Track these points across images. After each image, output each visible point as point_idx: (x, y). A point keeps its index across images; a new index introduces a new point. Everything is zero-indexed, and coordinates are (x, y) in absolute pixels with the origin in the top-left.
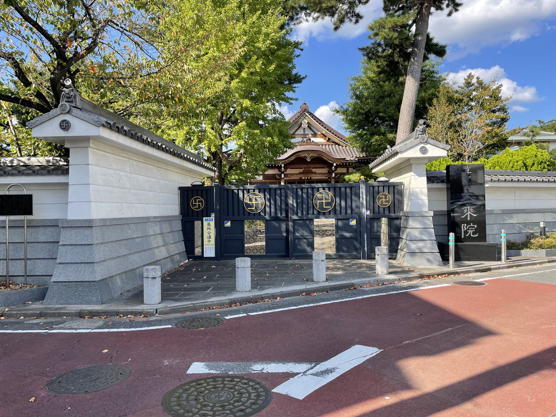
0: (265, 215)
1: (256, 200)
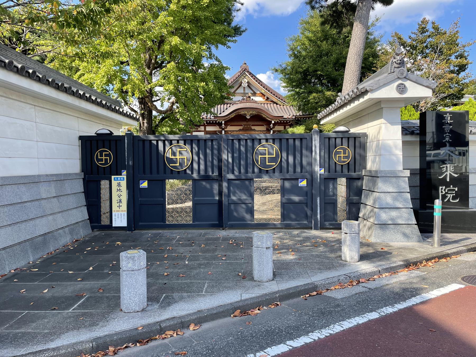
0: (192, 173)
1: (180, 153)
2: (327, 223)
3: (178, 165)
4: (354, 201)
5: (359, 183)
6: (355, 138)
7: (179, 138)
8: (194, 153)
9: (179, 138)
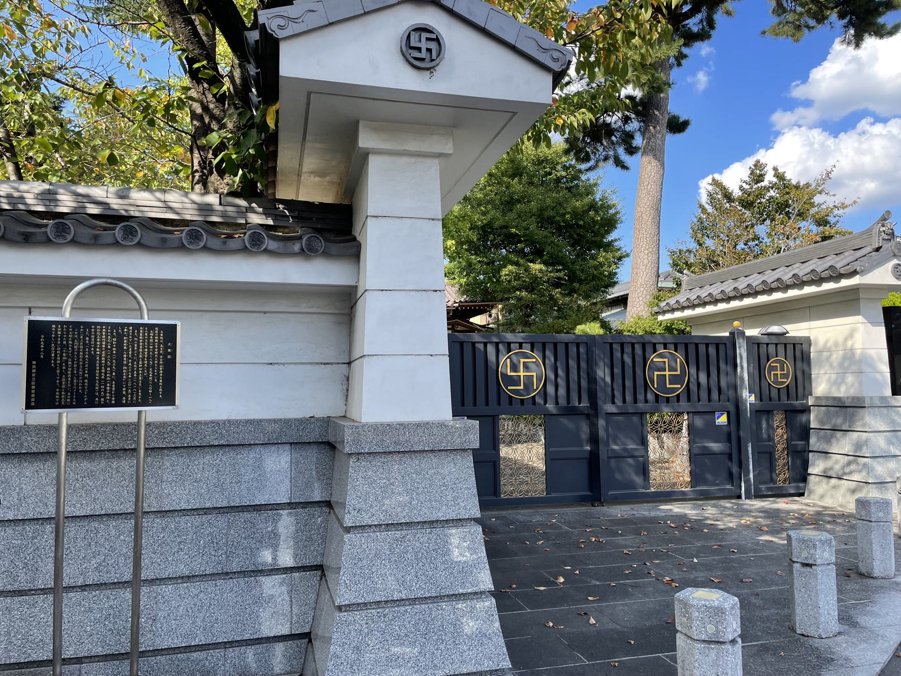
0: (545, 403)
1: (526, 367)
2: (763, 487)
3: (522, 387)
4: (799, 448)
5: (804, 418)
6: (794, 345)
7: (524, 339)
8: (547, 367)
9: (524, 339)
